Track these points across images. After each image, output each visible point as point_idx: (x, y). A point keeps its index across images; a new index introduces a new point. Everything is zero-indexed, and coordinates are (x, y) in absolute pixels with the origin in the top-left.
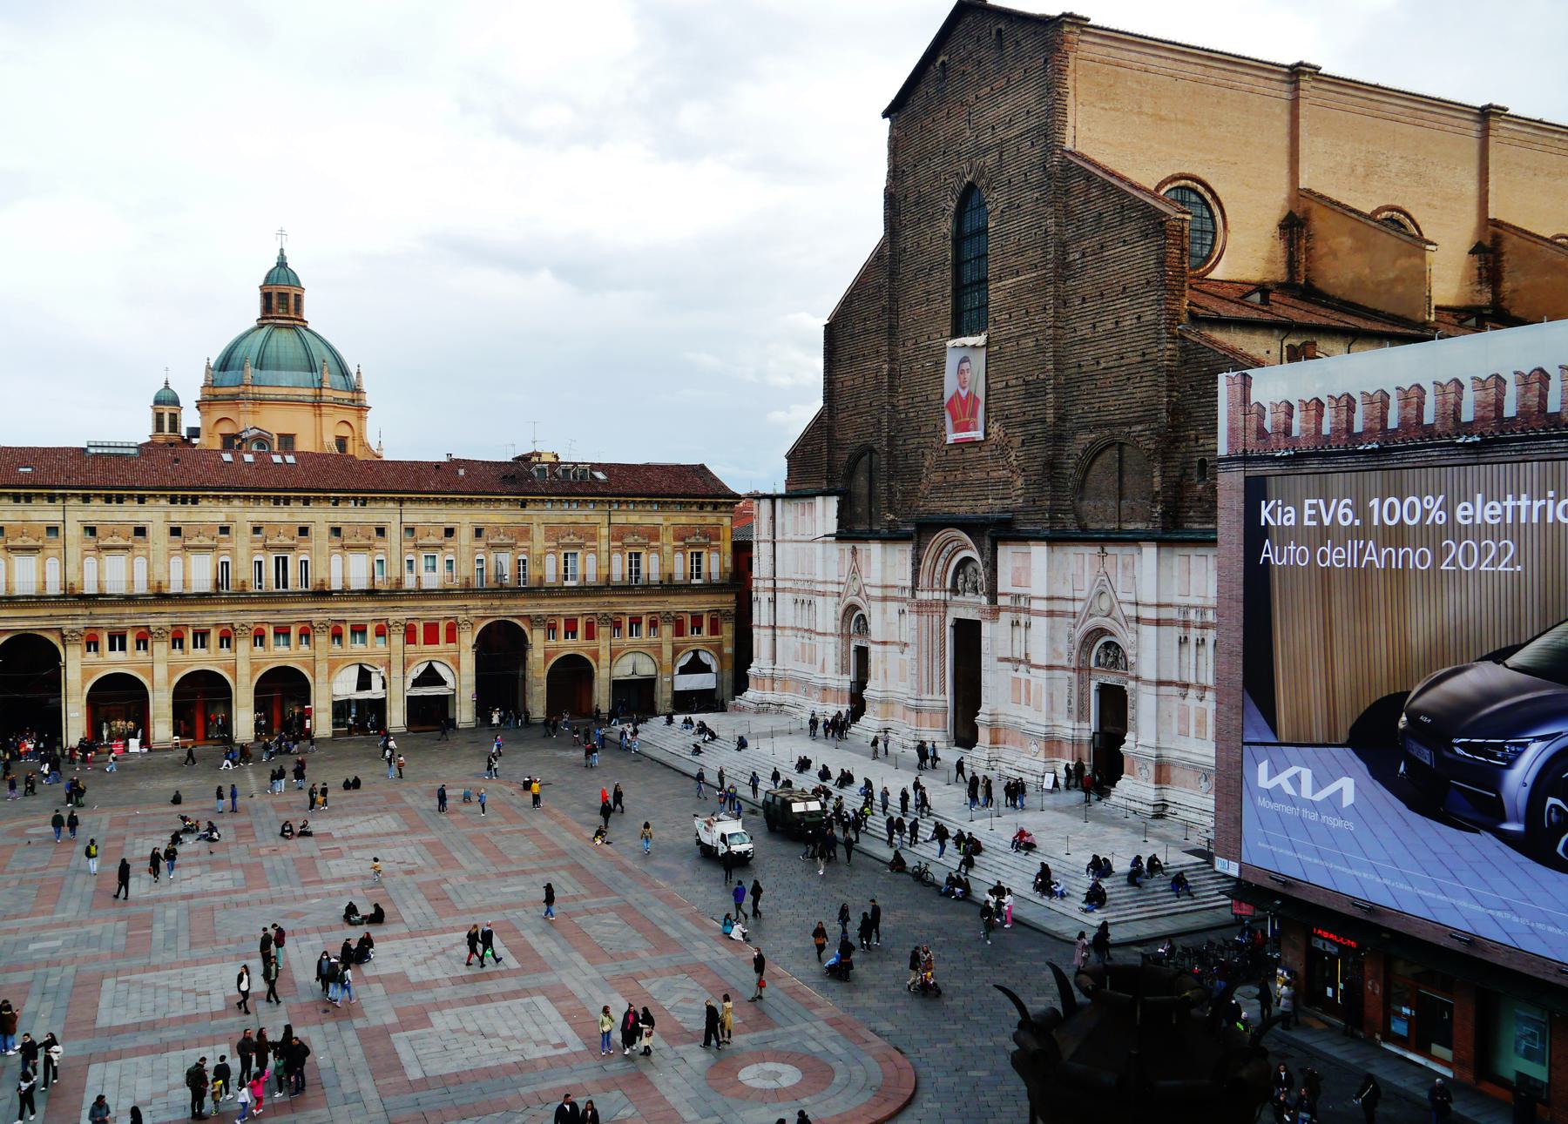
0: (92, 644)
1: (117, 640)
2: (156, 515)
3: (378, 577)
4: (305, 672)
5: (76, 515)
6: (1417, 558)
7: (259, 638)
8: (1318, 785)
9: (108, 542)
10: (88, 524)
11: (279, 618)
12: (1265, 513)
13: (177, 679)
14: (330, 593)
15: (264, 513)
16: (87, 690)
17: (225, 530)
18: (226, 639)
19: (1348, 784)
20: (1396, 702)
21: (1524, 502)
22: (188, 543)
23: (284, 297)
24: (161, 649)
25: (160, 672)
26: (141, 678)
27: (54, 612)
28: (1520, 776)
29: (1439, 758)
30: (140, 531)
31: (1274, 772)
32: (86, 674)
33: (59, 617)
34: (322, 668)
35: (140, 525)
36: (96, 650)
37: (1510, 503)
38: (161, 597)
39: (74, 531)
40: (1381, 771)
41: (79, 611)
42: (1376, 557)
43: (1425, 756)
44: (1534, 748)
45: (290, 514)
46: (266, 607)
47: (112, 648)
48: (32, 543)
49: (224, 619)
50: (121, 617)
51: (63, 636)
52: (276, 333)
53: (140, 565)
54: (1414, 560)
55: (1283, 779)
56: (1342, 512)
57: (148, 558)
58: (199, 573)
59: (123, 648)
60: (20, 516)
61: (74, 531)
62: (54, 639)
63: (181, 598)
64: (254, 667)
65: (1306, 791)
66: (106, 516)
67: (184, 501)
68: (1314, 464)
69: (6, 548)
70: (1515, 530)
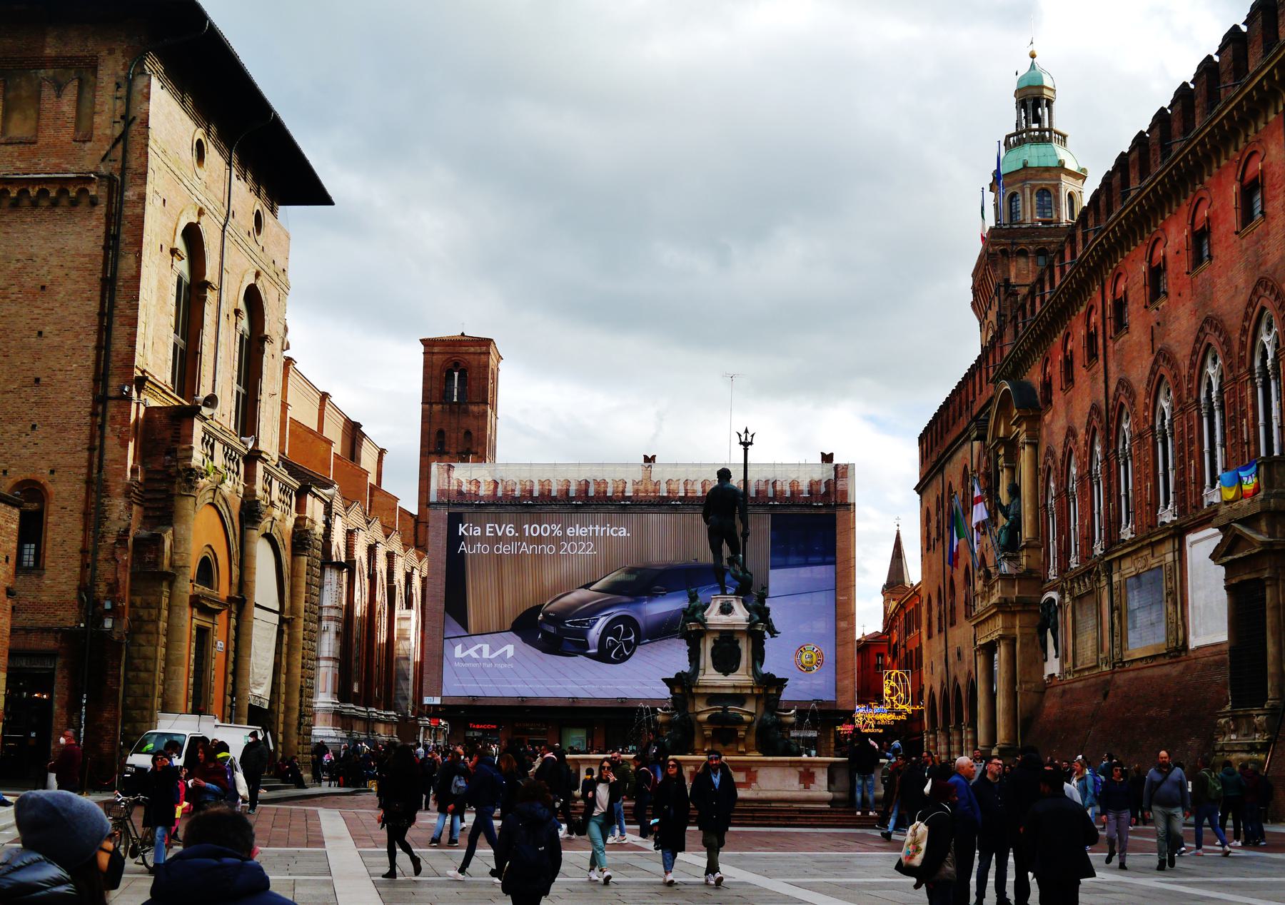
6: (548, 549)
8: (492, 650)
12: (461, 530)
19: (511, 647)
20: (538, 609)
21: (597, 528)
28: (595, 633)
29: (558, 629)
31: (465, 648)
37: (591, 528)
40: (526, 640)
42: (526, 548)
43: (552, 630)
44: (602, 619)
54: (547, 550)
55: (472, 652)
56: (509, 530)
65: (486, 654)
68: (493, 509)
70: (594, 538)
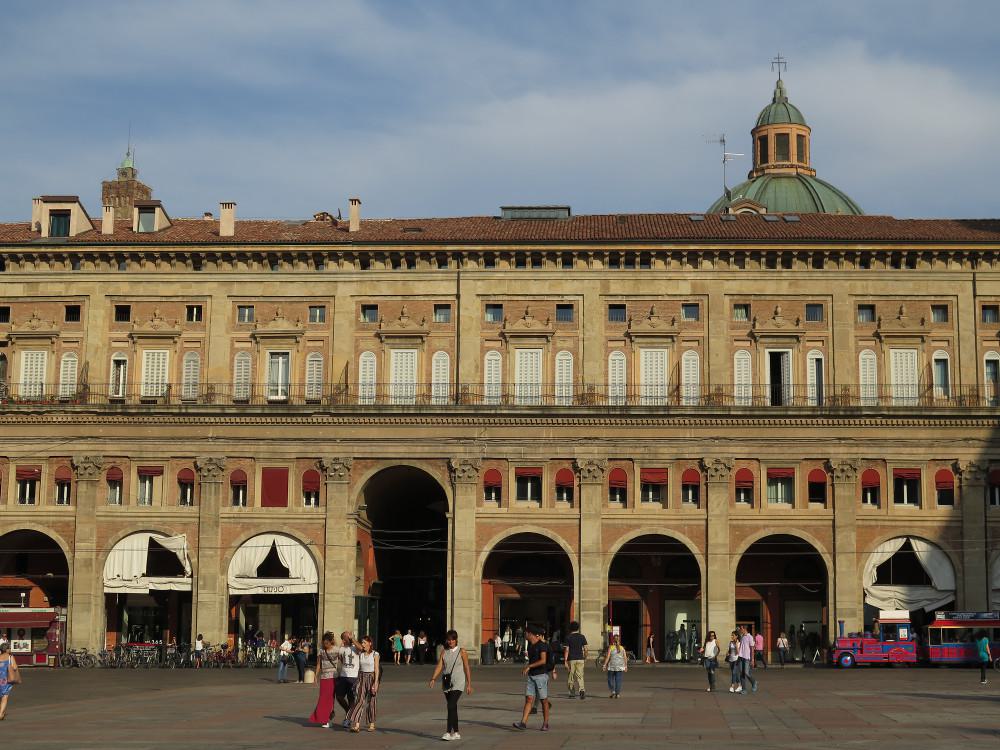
0: (493, 489)
1: (530, 483)
2: (589, 284)
3: (938, 392)
4: (819, 546)
5: (475, 285)
7: (745, 489)
9: (519, 326)
10: (493, 300)
11: (779, 455)
13: (616, 547)
14: (854, 414)
15: (753, 280)
16: (483, 557)
17: (692, 309)
18: (693, 488)
22: (634, 328)
23: (783, 139)
24: (593, 496)
25: (592, 534)
26: (562, 543)
27: (439, 432)
30: (565, 309)
32: (483, 532)
33: (447, 441)
34: (847, 539)
35: (566, 300)
36: (498, 498)
38: (589, 409)
39: (471, 310)
41: (475, 432)
45: (794, 282)
46: (755, 433)
47: (522, 495)
48: (412, 326)
49: (692, 451)
50: (535, 441)
51: (452, 470)
52: (773, 185)
53: (564, 362)
57: (575, 354)
58: (649, 372)
59: (537, 496)
60: (400, 289)
61: (471, 310)
62: (439, 475)
63: (625, 414)
64: (737, 531)
66: (517, 288)
67: (630, 263)
69: (378, 335)
